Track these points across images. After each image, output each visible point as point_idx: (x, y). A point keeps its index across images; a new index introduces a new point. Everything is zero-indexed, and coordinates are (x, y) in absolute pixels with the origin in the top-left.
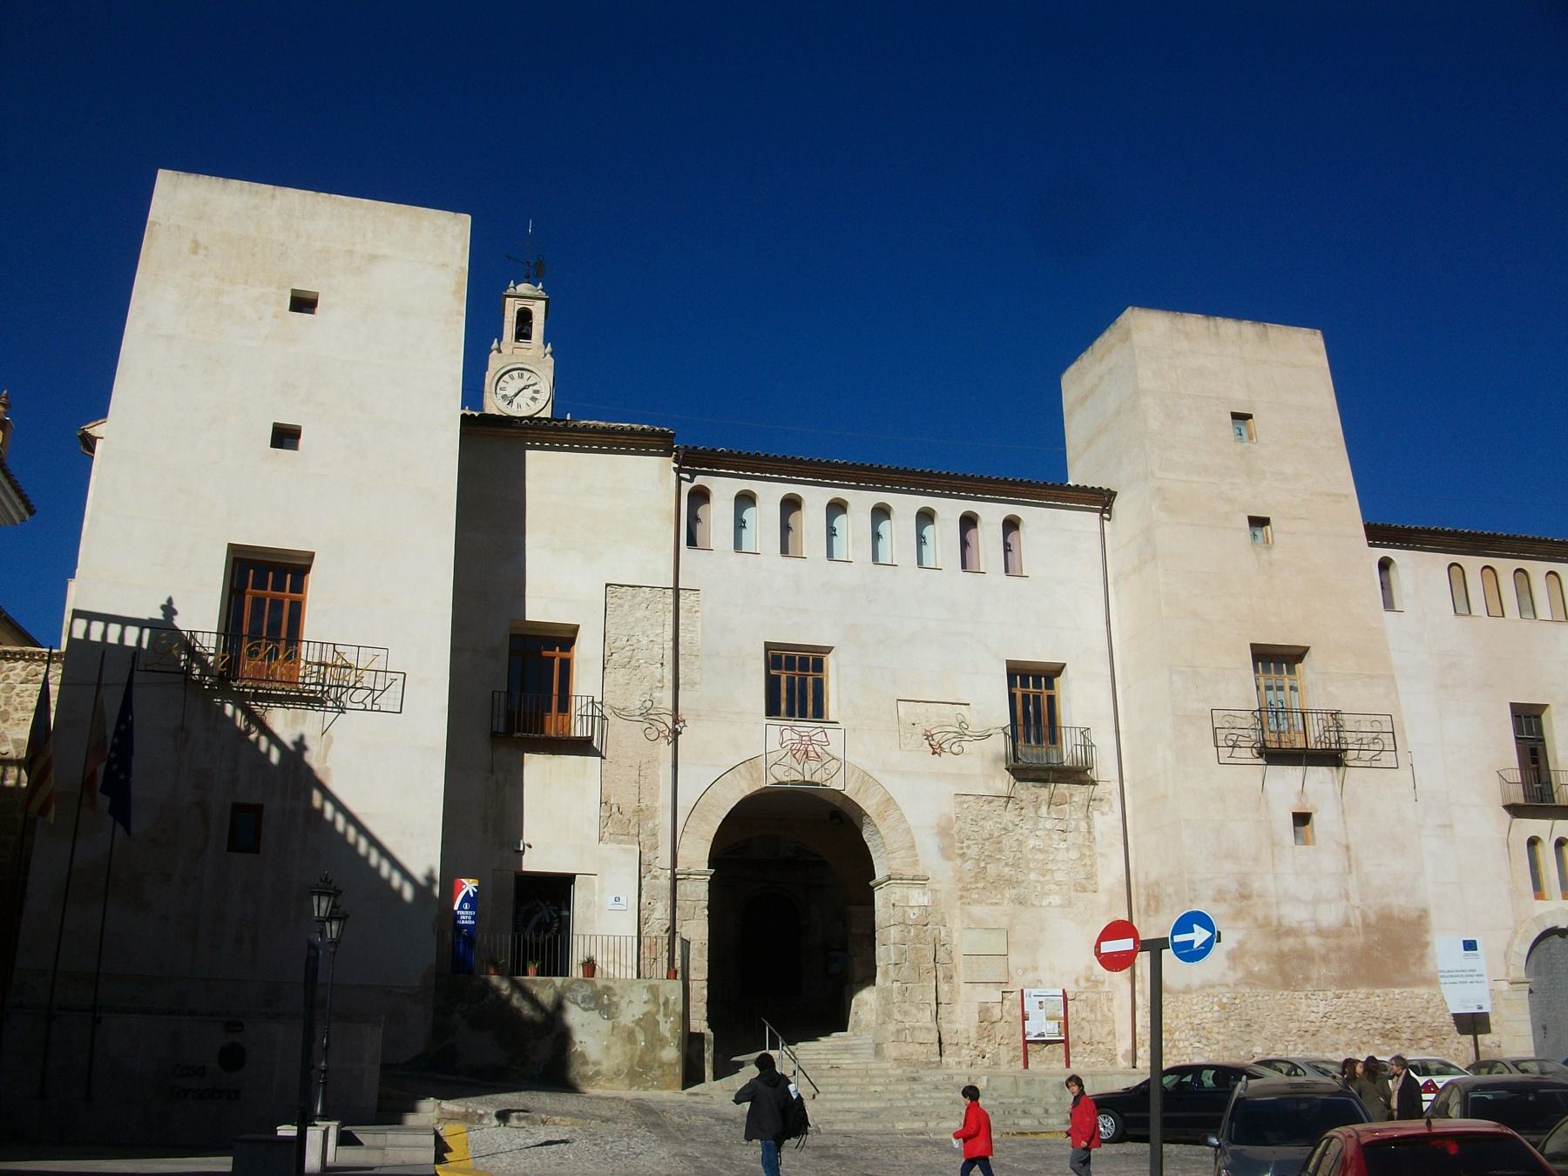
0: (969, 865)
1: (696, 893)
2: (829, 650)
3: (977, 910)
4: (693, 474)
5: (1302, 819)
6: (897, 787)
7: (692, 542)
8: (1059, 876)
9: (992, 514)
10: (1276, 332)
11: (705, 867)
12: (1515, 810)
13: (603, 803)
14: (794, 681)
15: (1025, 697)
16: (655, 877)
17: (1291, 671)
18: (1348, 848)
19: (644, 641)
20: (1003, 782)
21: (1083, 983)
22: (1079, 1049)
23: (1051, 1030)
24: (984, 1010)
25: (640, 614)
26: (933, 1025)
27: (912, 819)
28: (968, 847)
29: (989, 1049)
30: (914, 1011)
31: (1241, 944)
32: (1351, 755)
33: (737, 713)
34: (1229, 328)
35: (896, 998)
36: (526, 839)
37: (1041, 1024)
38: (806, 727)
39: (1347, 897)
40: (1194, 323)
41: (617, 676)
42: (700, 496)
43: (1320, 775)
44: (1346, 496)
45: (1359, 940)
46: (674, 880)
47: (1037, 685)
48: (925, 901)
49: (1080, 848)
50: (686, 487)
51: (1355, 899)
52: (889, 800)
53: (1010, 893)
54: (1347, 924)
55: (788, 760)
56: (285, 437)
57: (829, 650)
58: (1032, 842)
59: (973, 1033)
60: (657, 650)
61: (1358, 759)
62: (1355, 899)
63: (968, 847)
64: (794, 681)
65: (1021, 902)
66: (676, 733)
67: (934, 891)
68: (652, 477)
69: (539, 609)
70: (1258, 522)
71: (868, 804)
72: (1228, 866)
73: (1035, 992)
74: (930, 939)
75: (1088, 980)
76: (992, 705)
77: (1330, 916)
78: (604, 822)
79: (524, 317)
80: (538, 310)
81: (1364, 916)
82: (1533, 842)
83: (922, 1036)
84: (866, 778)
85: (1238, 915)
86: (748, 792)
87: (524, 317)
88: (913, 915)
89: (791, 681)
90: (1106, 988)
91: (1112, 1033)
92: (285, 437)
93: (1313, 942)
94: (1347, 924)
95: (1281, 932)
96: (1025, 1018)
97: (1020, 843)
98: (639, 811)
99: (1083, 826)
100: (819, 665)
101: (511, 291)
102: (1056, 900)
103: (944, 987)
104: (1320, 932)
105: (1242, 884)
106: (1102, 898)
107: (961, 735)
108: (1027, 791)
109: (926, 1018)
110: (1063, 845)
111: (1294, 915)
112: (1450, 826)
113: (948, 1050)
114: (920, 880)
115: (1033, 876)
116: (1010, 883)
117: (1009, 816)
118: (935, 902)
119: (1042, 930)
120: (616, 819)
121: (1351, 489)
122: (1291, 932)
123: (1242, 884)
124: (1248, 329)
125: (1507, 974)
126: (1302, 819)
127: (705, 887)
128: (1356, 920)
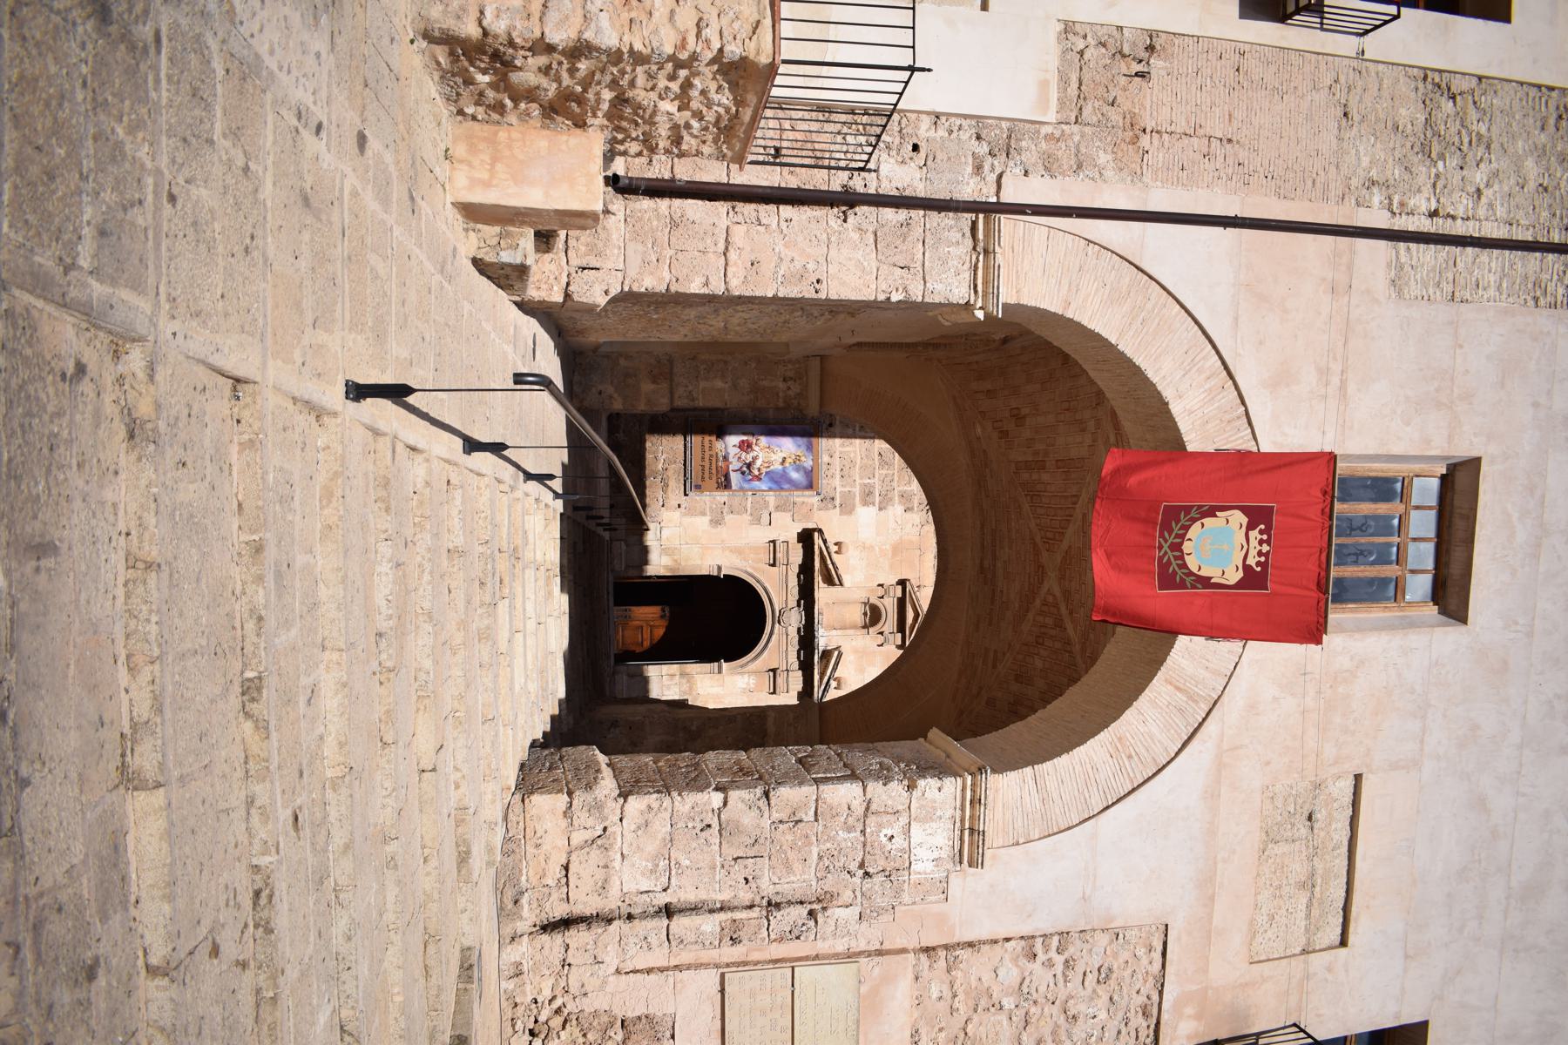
3: (900, 996)
11: (1007, 295)
16: (978, 169)
19: (1479, 177)
25: (1531, 167)
26: (611, 903)
28: (1049, 964)
30: (651, 847)
33: (1343, 386)
35: (686, 802)
48: (924, 865)
59: (588, 1005)
60: (1462, 205)
63: (1049, 964)
74: (829, 884)
83: (585, 869)
86: (1176, 409)
98: (1136, 130)
103: (710, 925)
109: (633, 879)
114: (971, 845)
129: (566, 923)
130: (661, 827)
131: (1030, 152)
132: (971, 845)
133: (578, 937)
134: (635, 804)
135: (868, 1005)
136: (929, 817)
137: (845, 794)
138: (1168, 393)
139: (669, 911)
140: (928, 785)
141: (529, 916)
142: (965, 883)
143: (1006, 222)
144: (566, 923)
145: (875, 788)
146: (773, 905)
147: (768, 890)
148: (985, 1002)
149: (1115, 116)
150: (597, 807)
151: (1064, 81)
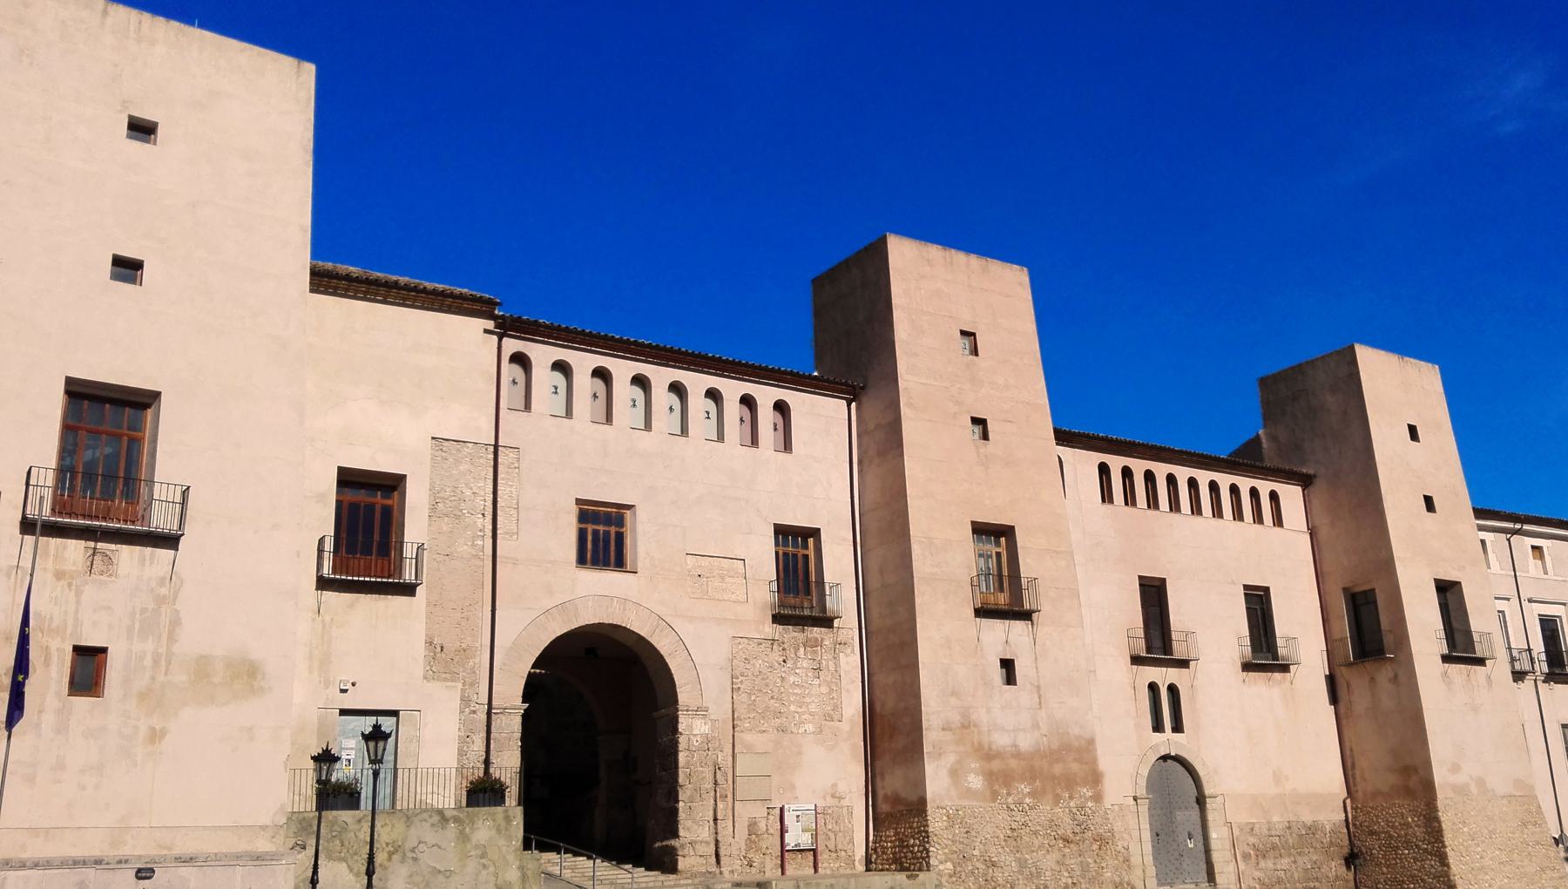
1: (510, 726)
5: (1008, 665)
8: (813, 708)
10: (997, 268)
13: (430, 643)
15: (786, 554)
17: (998, 544)
20: (770, 629)
21: (829, 799)
22: (825, 856)
23: (805, 840)
24: (752, 826)
29: (757, 859)
34: (960, 257)
37: (797, 836)
40: (934, 251)
46: (489, 714)
47: (795, 545)
48: (706, 729)
49: (829, 684)
56: (127, 268)
58: (792, 679)
65: (782, 730)
70: (979, 422)
71: (663, 645)
73: (793, 807)
74: (710, 763)
75: (833, 796)
83: (701, 849)
89: (595, 533)
90: (845, 803)
91: (851, 841)
92: (127, 268)
96: (783, 831)
99: (832, 668)
100: (620, 521)
102: (810, 727)
103: (720, 805)
106: (845, 727)
108: (791, 634)
109: (705, 833)
110: (816, 682)
113: (723, 860)
114: (701, 711)
115: (792, 708)
117: (776, 656)
119: (800, 753)
120: (441, 658)
121: (1044, 400)
124: (974, 261)
126: (1008, 665)
127: (519, 720)
129: (717, 856)
130: (689, 823)
131: (470, 692)
132: (701, 711)
133: (722, 852)
134: (682, 833)
135: (750, 749)
136: (690, 727)
137: (682, 757)
138: (554, 637)
139: (715, 820)
140: (681, 728)
141: (714, 869)
142: (714, 713)
143: (494, 703)
144: (717, 856)
145: (681, 747)
146: (716, 783)
147: (711, 785)
148: (752, 706)
149: (457, 659)
150: (682, 846)
151: (445, 680)
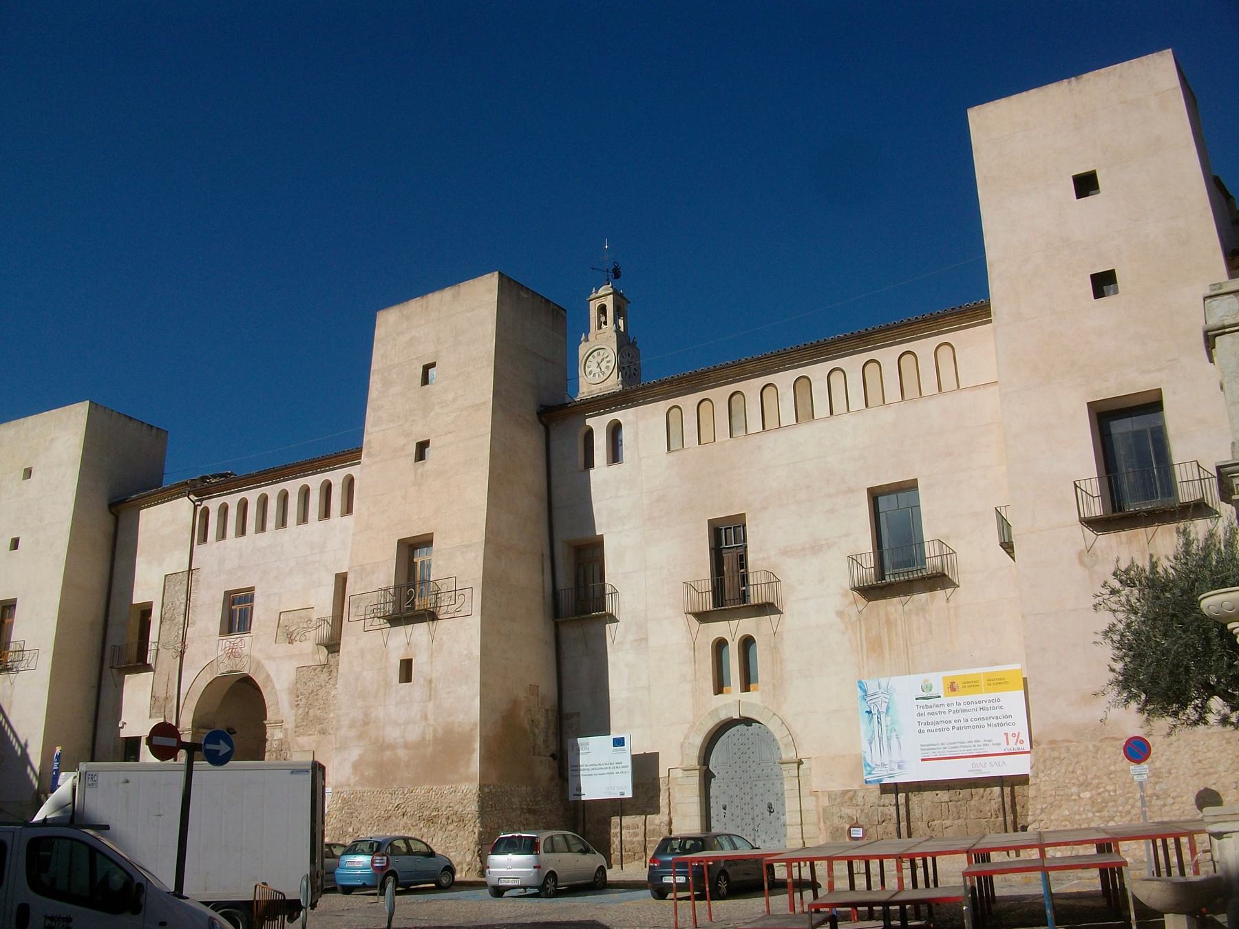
0: (300, 711)
2: (252, 589)
4: (201, 501)
6: (270, 667)
7: (204, 539)
9: (336, 477)
11: (190, 726)
12: (703, 617)
14: (237, 612)
18: (430, 681)
27: (277, 686)
31: (361, 756)
32: (443, 610)
34: (435, 298)
36: (123, 720)
38: (234, 638)
39: (426, 718)
40: (415, 305)
41: (166, 626)
42: (206, 513)
43: (420, 631)
44: (484, 403)
45: (430, 750)
50: (199, 509)
51: (431, 721)
52: (268, 676)
53: (318, 727)
54: (424, 739)
55: (226, 661)
57: (252, 589)
61: (447, 612)
62: (431, 721)
64: (237, 612)
65: (323, 732)
66: (182, 653)
67: (286, 730)
68: (181, 509)
69: (138, 597)
71: (259, 680)
72: (360, 703)
76: (323, 602)
77: (413, 735)
78: (152, 707)
79: (603, 309)
80: (609, 302)
81: (435, 731)
82: (720, 645)
84: (259, 666)
85: (361, 736)
87: (603, 309)
88: (275, 744)
93: (401, 753)
94: (424, 739)
95: (383, 746)
97: (328, 693)
100: (251, 599)
101: (592, 297)
104: (406, 746)
105: (366, 715)
107: (306, 630)
111: (393, 734)
112: (646, 639)
116: (320, 720)
117: (324, 676)
118: (286, 735)
122: (392, 747)
123: (366, 715)
124: (447, 294)
125: (682, 763)
128: (429, 736)
